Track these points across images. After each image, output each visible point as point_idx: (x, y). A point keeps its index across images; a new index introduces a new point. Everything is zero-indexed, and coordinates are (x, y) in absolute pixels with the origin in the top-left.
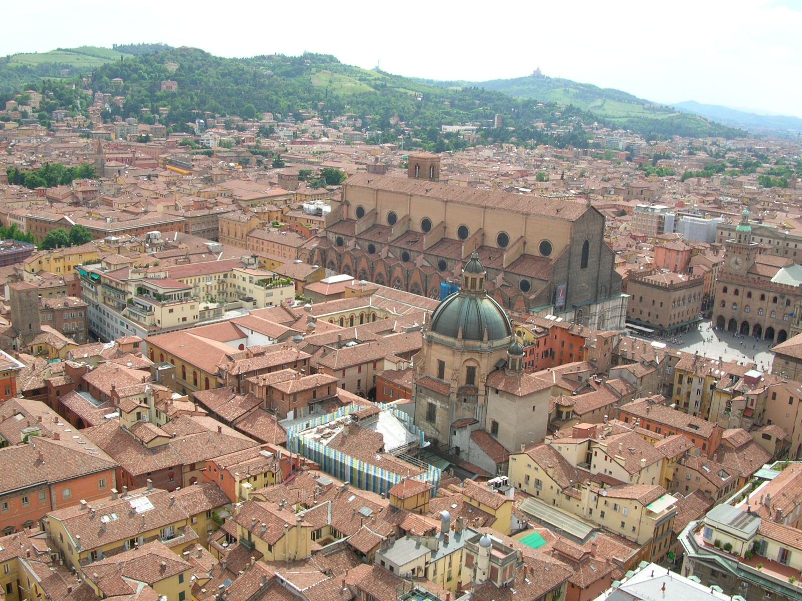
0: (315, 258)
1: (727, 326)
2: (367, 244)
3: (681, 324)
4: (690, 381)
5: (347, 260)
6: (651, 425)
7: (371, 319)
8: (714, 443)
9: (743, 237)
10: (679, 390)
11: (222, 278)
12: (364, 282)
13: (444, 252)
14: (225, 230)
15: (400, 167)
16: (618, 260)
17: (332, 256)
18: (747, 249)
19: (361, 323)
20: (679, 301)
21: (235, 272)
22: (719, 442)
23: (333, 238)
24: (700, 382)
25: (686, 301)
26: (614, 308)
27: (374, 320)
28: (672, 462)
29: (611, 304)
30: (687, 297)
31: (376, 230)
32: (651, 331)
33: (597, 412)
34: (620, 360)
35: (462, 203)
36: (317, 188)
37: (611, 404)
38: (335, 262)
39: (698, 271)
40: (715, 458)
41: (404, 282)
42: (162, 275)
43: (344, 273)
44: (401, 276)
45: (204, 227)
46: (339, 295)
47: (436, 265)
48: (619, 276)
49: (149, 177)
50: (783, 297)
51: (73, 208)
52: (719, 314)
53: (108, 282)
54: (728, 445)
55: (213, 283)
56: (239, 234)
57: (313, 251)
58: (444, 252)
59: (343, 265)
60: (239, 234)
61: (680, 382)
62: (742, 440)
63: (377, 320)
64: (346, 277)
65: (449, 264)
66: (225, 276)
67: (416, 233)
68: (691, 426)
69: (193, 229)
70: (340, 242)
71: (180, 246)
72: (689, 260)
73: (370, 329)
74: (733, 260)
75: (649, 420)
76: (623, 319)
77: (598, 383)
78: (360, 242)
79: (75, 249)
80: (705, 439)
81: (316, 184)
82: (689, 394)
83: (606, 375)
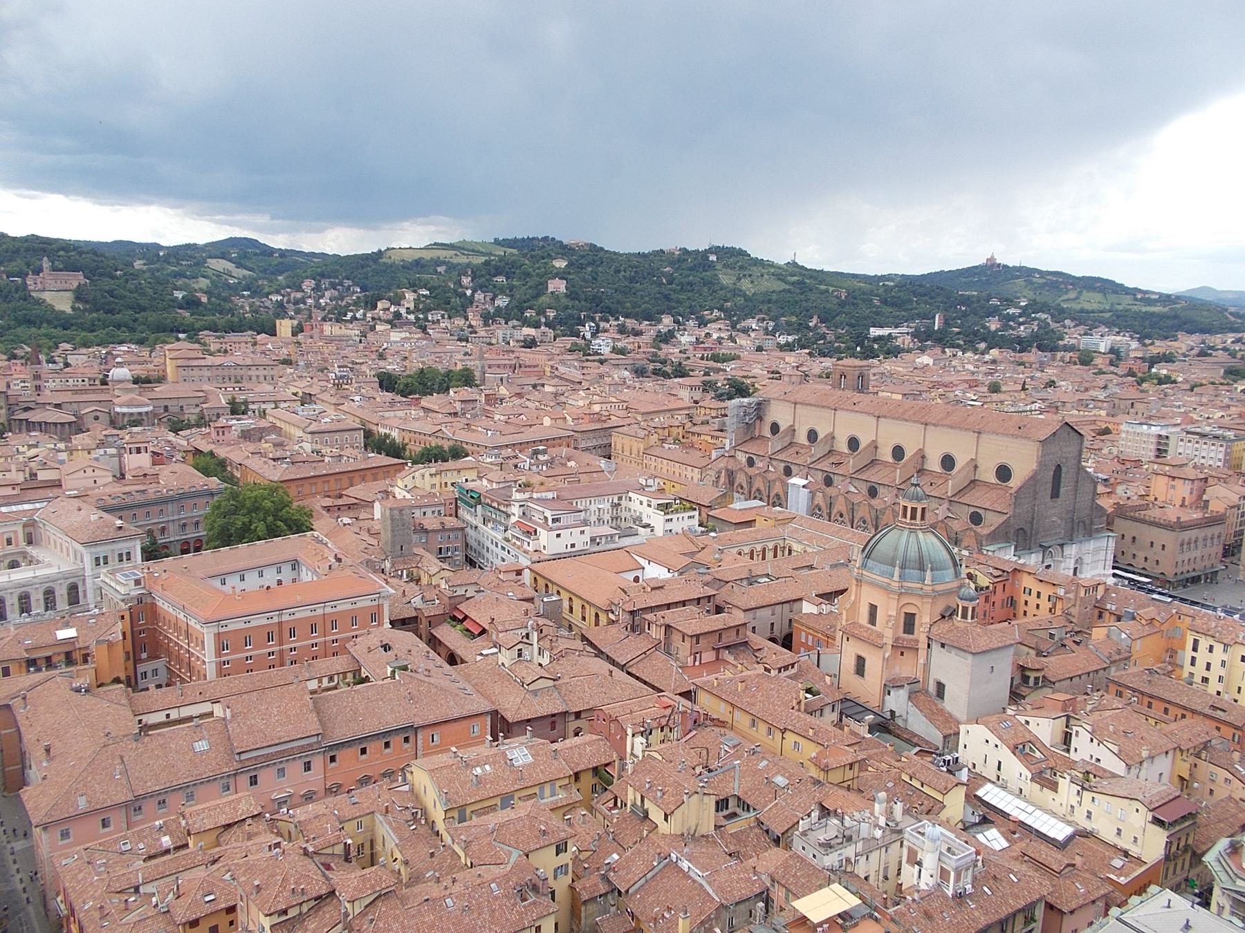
0: (722, 480)
2: (783, 465)
5: (758, 484)
7: (787, 552)
11: (616, 501)
12: (778, 508)
13: (873, 476)
14: (619, 447)
15: (820, 377)
17: (741, 479)
19: (775, 556)
21: (631, 494)
23: (742, 458)
27: (790, 553)
31: (792, 450)
35: (897, 419)
36: (723, 400)
38: (745, 486)
41: (825, 511)
42: (550, 495)
43: (755, 498)
44: (822, 504)
45: (595, 443)
46: (750, 523)
47: (864, 491)
49: (534, 386)
51: (450, 419)
53: (488, 501)
55: (606, 506)
56: (635, 451)
57: (719, 472)
58: (873, 476)
59: (753, 490)
60: (635, 451)
63: (794, 554)
64: (757, 503)
65: (881, 490)
66: (620, 498)
67: (840, 454)
69: (583, 445)
70: (751, 463)
71: (569, 464)
73: (785, 565)
78: (774, 463)
79: (451, 464)
81: (722, 395)
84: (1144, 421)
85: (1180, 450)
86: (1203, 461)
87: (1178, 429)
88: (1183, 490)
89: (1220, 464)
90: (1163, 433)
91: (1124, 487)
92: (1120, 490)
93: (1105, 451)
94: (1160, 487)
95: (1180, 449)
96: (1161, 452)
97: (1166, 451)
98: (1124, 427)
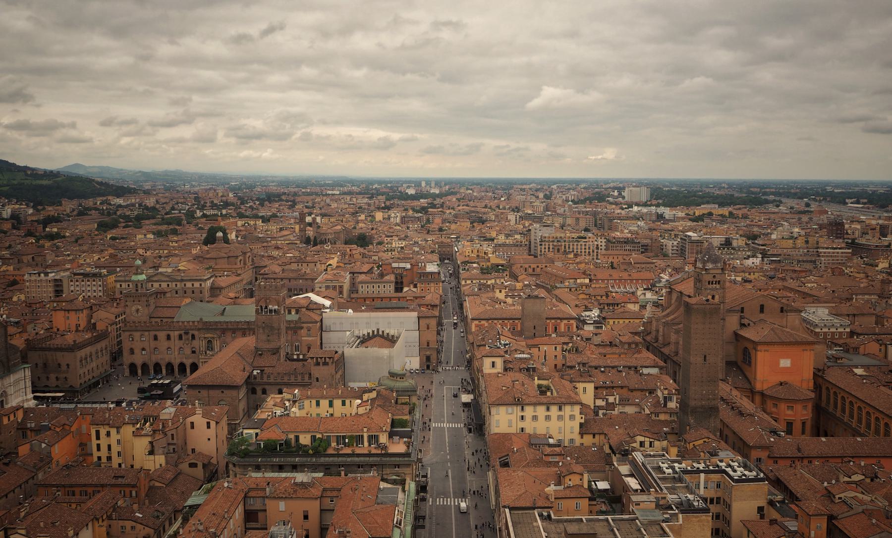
1: (140, 371)
3: (94, 381)
4: (108, 434)
6: (77, 490)
8: (142, 487)
9: (139, 285)
10: (98, 446)
16: (11, 330)
18: (145, 295)
20: (86, 359)
22: (147, 486)
24: (118, 432)
25: (94, 357)
26: (17, 382)
28: (103, 521)
29: (13, 378)
30: (94, 353)
32: (61, 394)
33: (11, 496)
34: (29, 433)
37: (27, 482)
39: (100, 326)
40: (147, 501)
48: (14, 347)
50: (186, 333)
52: (130, 362)
54: (157, 484)
61: (98, 438)
62: (170, 475)
68: (116, 477)
72: (90, 317)
74: (134, 308)
75: (71, 486)
76: (29, 390)
77: (6, 464)
80: (134, 486)
82: (109, 447)
83: (14, 453)
84: (41, 270)
85: (72, 288)
86: (89, 294)
87: (67, 273)
88: (82, 319)
89: (101, 294)
90: (58, 277)
91: (33, 325)
92: (30, 328)
93: (15, 299)
94: (60, 320)
95: (71, 288)
96: (58, 292)
97: (62, 291)
98: (26, 277)
